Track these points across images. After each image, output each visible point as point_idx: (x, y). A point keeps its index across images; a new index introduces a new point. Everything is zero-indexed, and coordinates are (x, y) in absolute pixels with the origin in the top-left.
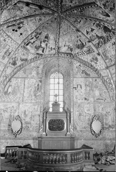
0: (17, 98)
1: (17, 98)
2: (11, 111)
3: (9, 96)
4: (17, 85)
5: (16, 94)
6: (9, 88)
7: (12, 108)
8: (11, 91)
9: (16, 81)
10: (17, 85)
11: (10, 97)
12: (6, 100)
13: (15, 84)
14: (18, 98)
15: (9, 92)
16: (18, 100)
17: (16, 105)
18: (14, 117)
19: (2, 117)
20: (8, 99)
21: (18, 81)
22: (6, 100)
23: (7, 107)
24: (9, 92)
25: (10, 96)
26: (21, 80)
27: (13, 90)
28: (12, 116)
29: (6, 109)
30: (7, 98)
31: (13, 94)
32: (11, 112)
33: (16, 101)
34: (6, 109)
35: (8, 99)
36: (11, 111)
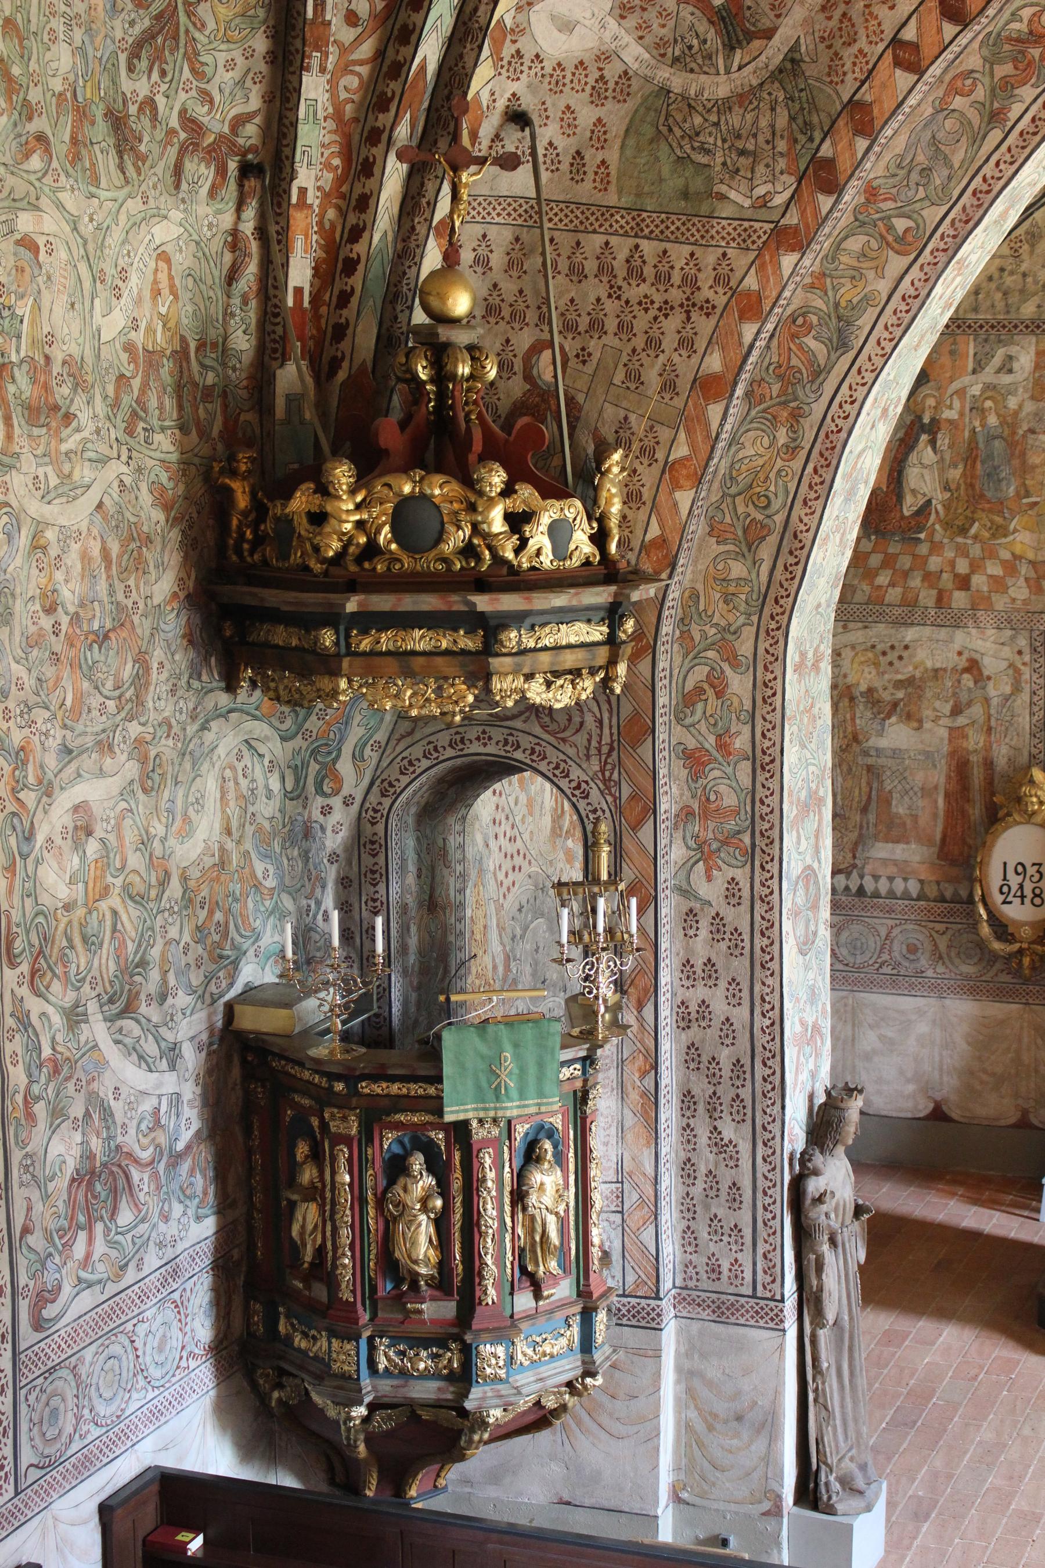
0: (1011, 567)
1: (1011, 567)
2: (956, 711)
3: (923, 549)
4: (992, 420)
5: (1000, 531)
6: (913, 458)
7: (967, 680)
8: (939, 497)
9: (988, 375)
10: (992, 420)
11: (934, 563)
12: (894, 594)
13: (976, 408)
14: (1024, 569)
15: (909, 505)
16: (1019, 591)
17: (1007, 652)
18: (990, 781)
19: (869, 768)
20: (916, 582)
21: (1007, 367)
22: (894, 594)
23: (906, 671)
24: (909, 505)
25: (936, 548)
26: (1038, 354)
27: (955, 474)
28: (977, 776)
29: (900, 694)
30: (906, 574)
31: (963, 531)
32: (961, 721)
33: (1000, 602)
34: (900, 694)
35: (916, 582)
36: (956, 711)
